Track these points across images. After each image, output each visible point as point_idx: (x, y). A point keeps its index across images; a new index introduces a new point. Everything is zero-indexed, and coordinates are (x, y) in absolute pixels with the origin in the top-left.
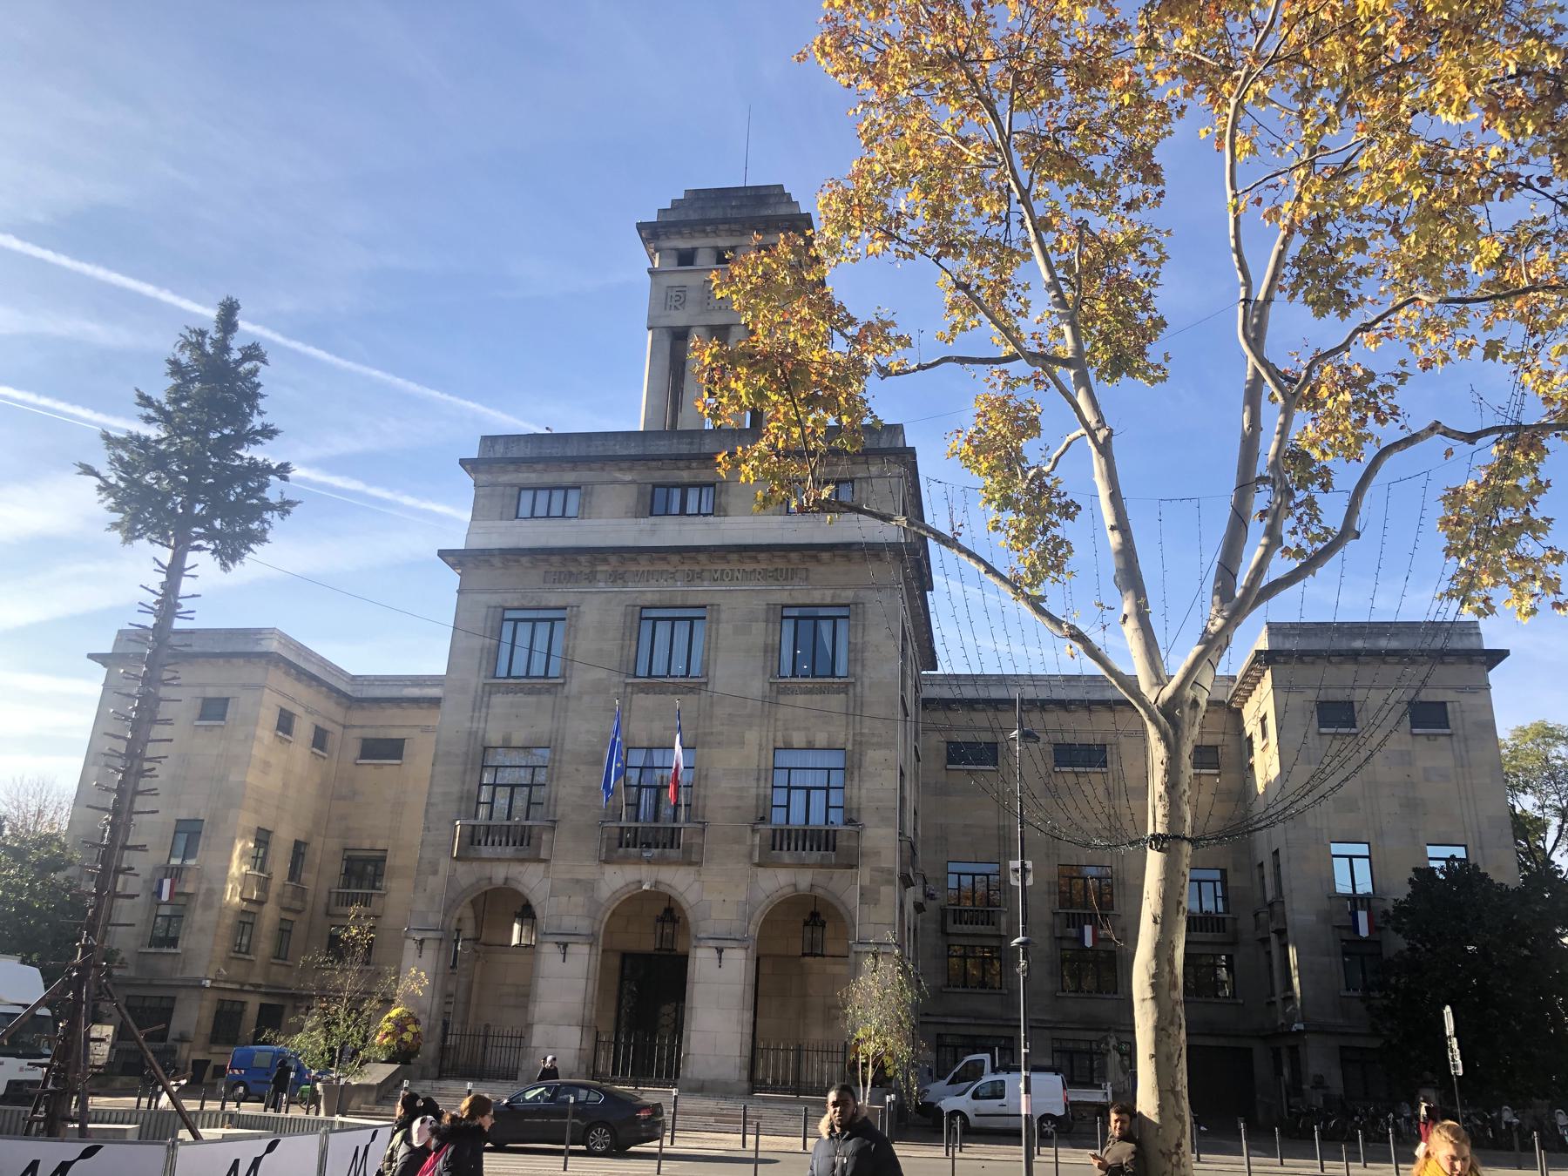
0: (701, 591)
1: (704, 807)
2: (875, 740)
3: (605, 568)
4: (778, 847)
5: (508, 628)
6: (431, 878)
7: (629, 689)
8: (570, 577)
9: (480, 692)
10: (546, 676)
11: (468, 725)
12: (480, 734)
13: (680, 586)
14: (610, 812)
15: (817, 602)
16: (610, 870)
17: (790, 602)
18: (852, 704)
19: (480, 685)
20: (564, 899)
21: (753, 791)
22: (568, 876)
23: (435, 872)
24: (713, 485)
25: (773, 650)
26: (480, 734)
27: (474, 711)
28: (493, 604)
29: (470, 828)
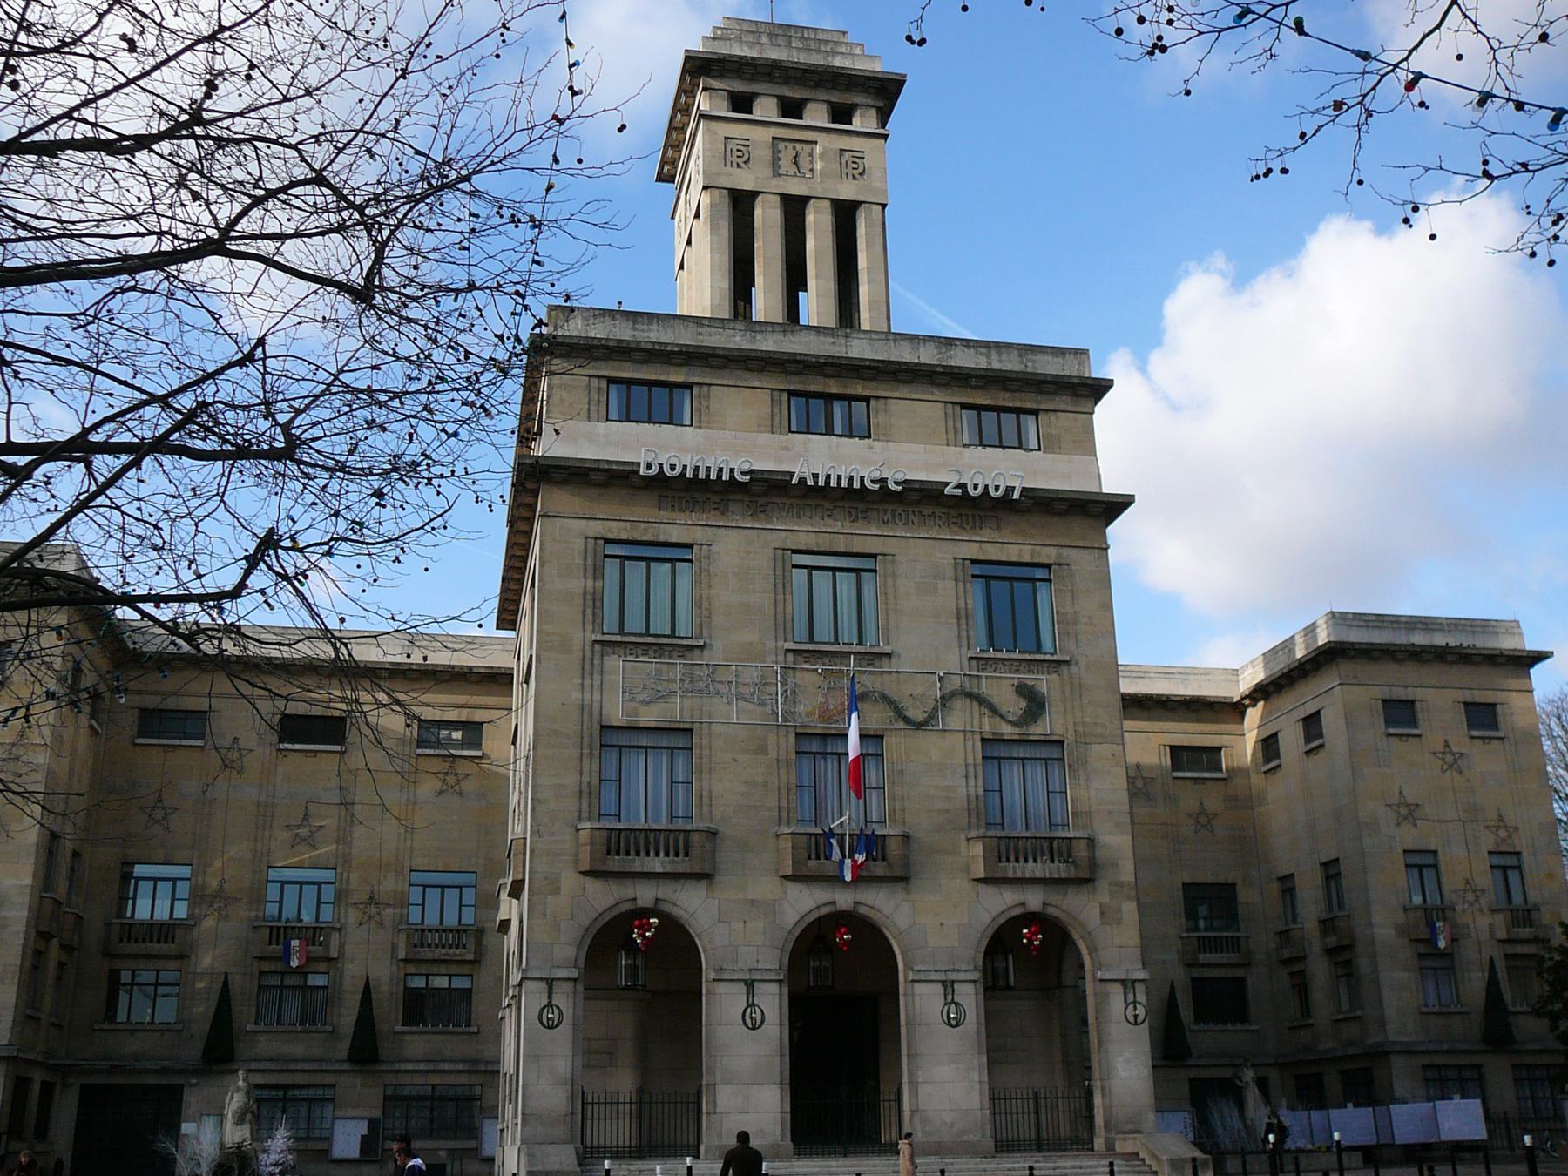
0: (866, 535)
1: (903, 810)
2: (1099, 730)
3: (739, 497)
4: (1004, 859)
5: (611, 568)
6: (549, 897)
7: (790, 657)
8: (693, 505)
9: (588, 655)
10: (673, 635)
11: (577, 695)
12: (596, 706)
13: (838, 526)
14: (784, 815)
15: (1014, 559)
16: (794, 889)
17: (982, 557)
18: (1068, 689)
19: (588, 643)
20: (738, 925)
21: (962, 792)
22: (741, 896)
23: (556, 891)
24: (867, 399)
25: (962, 616)
26: (596, 706)
27: (583, 679)
28: (591, 535)
29: (605, 833)
